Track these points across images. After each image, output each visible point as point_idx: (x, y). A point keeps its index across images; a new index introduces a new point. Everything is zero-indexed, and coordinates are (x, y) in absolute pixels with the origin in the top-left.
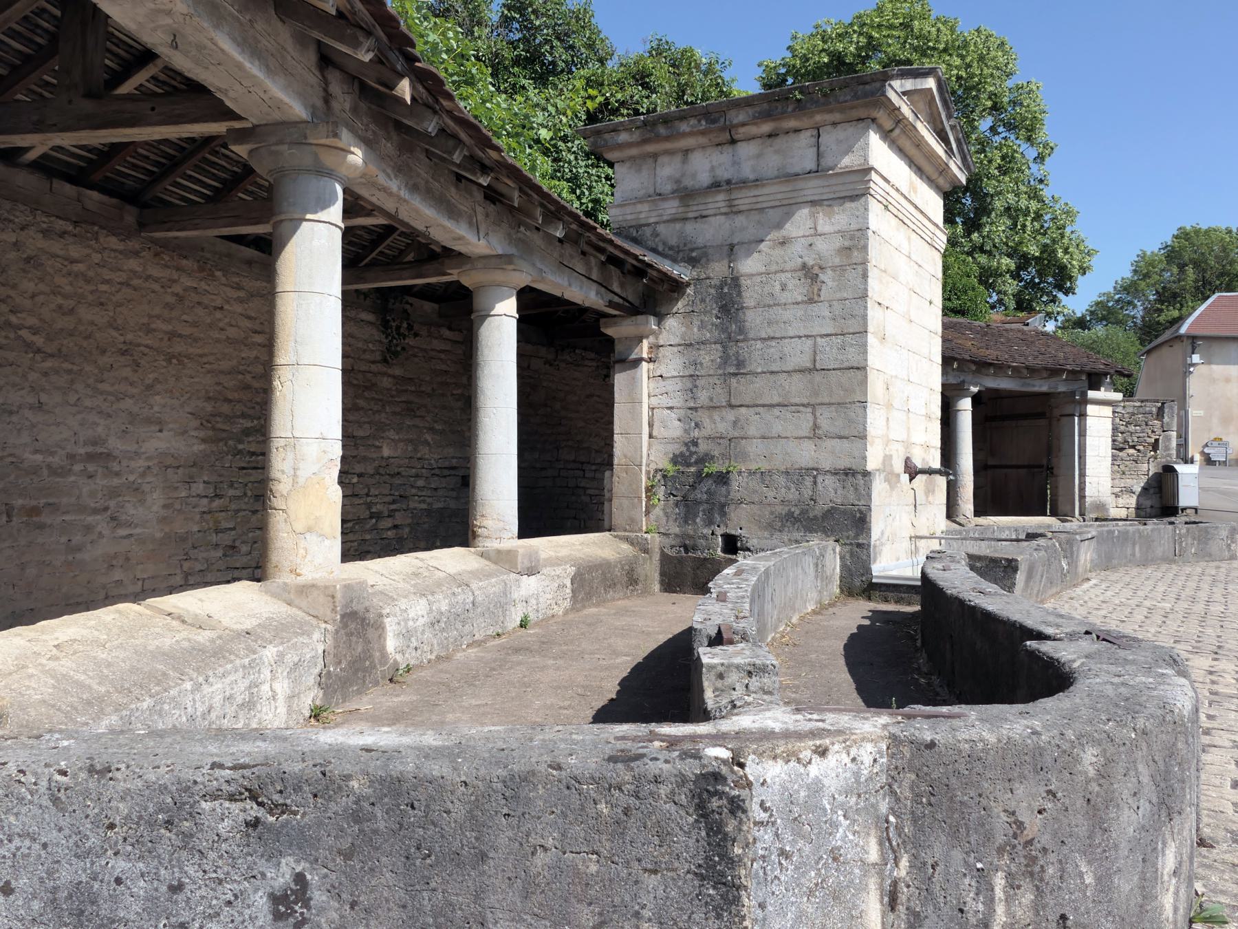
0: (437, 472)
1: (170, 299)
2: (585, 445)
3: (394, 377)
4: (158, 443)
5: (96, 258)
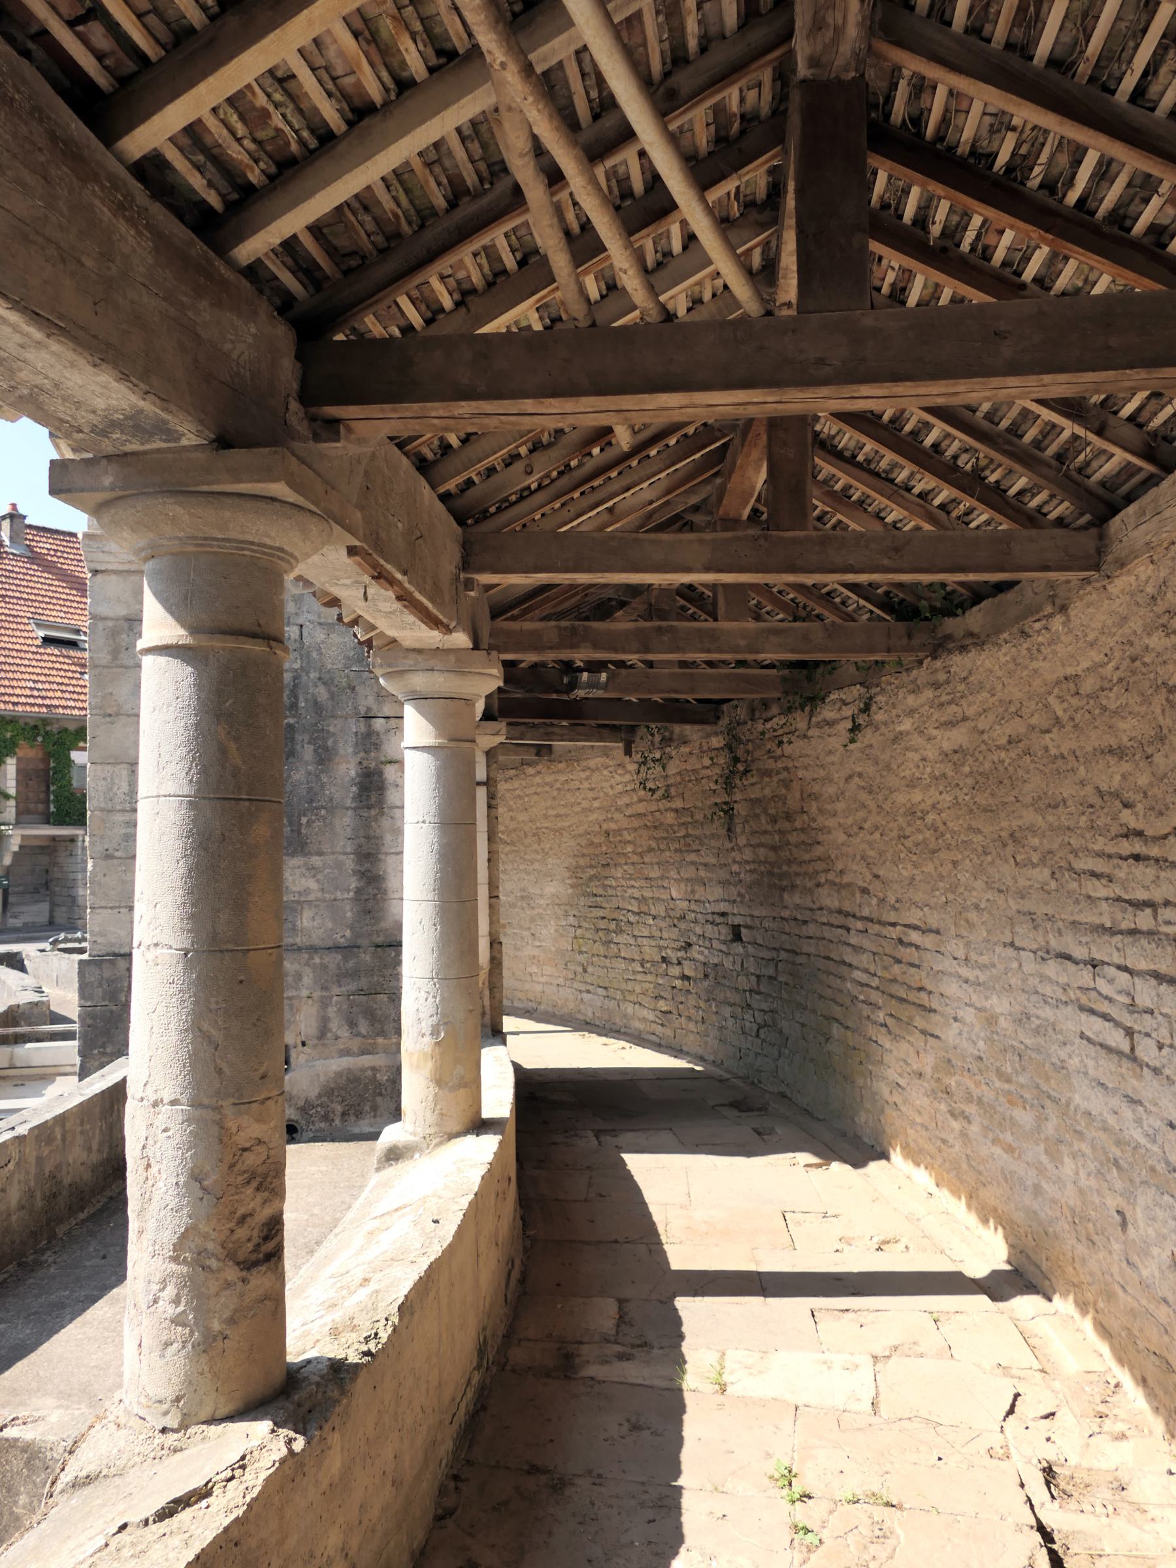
0: (710, 917)
1: (555, 793)
2: (846, 879)
3: (676, 811)
4: (551, 888)
5: (524, 783)
